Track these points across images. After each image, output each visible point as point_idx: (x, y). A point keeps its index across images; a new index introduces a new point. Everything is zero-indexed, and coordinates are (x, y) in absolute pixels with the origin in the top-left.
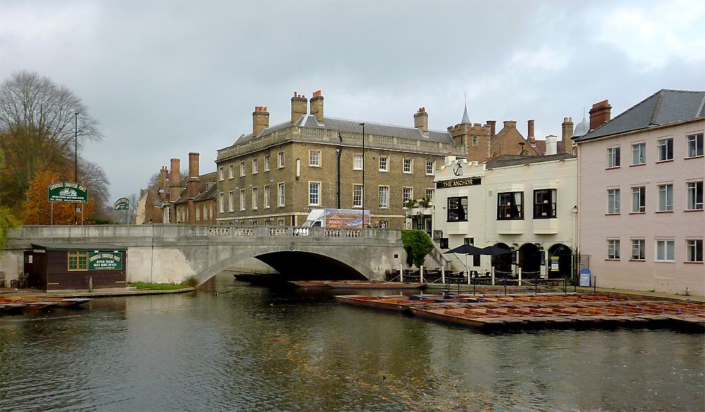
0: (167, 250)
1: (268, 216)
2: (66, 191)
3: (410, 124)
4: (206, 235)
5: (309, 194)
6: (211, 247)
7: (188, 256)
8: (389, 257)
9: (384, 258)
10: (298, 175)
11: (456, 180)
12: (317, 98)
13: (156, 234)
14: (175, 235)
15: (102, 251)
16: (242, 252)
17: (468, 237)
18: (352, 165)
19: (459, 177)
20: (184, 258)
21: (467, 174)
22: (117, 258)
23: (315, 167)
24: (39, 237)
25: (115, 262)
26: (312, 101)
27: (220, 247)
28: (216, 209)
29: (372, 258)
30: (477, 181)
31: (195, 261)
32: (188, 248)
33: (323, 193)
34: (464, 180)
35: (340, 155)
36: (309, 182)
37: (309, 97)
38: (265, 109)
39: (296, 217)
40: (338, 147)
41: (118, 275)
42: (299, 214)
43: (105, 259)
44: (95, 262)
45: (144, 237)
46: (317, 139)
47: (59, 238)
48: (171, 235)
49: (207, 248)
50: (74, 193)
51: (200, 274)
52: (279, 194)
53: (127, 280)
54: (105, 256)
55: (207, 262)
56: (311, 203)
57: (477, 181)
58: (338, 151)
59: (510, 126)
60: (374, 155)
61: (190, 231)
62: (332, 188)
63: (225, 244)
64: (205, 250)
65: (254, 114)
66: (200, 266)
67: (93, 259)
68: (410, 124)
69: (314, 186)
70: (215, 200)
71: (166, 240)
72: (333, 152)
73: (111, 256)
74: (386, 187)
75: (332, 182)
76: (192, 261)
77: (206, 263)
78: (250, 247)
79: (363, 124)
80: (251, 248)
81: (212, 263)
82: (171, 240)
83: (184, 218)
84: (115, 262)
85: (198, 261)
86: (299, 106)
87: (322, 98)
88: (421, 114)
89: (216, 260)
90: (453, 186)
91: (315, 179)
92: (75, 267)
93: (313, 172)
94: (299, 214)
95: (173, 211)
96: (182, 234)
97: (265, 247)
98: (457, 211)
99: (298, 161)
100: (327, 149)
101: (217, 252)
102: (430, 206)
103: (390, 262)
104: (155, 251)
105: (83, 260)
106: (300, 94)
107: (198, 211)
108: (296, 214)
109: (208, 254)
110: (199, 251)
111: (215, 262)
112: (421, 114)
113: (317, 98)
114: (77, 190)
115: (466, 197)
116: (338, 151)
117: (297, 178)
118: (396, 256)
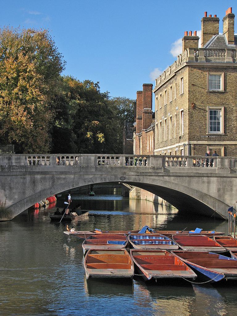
1: (175, 146)
4: (23, 164)
6: (28, 178)
27: (38, 177)
42: (195, 142)
46: (217, 61)
49: (25, 178)
52: (181, 122)
55: (24, 193)
56: (211, 130)
64: (22, 180)
66: (16, 197)
69: (214, 114)
76: (7, 192)
78: (72, 176)
80: (74, 178)
81: (29, 193)
83: (151, 150)
85: (14, 191)
86: (210, 27)
89: (34, 190)
91: (216, 104)
93: (213, 96)
94: (195, 142)
95: (138, 142)
97: (91, 176)
101: (34, 182)
106: (212, 13)
107: (148, 142)
108: (192, 142)
109: (24, 183)
110: (15, 181)
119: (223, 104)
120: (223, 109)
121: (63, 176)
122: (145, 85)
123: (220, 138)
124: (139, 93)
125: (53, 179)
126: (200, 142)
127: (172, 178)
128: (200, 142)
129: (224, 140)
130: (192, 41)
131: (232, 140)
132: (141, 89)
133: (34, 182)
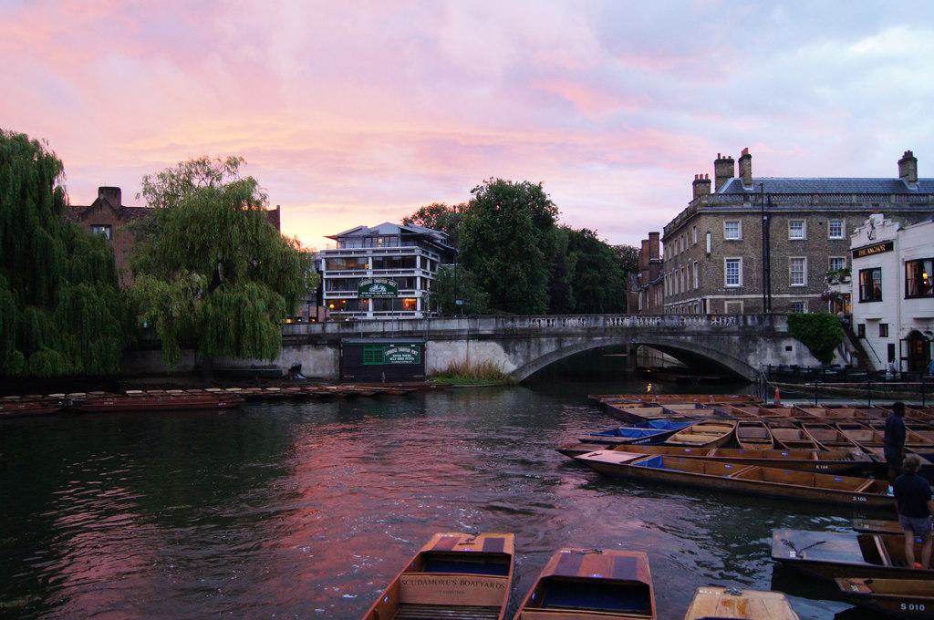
0: (482, 343)
2: (376, 287)
3: (894, 173)
5: (726, 273)
7: (507, 350)
8: (777, 350)
9: (769, 351)
10: (709, 250)
11: (872, 246)
12: (746, 157)
13: (472, 327)
14: (492, 328)
15: (398, 345)
16: (570, 344)
17: (883, 322)
18: (787, 233)
19: (872, 242)
20: (502, 351)
21: (881, 236)
22: (415, 352)
23: (732, 241)
24: (355, 331)
25: (413, 355)
26: (740, 160)
27: (544, 340)
28: (663, 293)
29: (751, 351)
30: (888, 246)
31: (515, 354)
32: (506, 339)
33: (746, 271)
34: (878, 245)
35: (768, 223)
36: (725, 259)
37: (736, 156)
38: (707, 175)
39: (708, 301)
40: (764, 214)
41: (418, 366)
42: (711, 297)
43: (402, 353)
44: (391, 355)
45: (459, 330)
47: (374, 333)
48: (487, 327)
50: (383, 289)
51: (521, 369)
52: (695, 274)
53: (428, 372)
54: (401, 350)
55: (528, 357)
56: (729, 283)
57: (888, 246)
58: (765, 218)
59: (701, 176)
60: (823, 219)
61: (510, 323)
62: (756, 266)
63: (549, 335)
65: (695, 183)
66: (521, 361)
67: (391, 352)
68: (894, 173)
69: (732, 263)
70: (663, 285)
71: (483, 333)
72: (758, 220)
73: (409, 350)
74: (841, 259)
75: (755, 254)
76: (512, 355)
77: (528, 357)
79: (762, 184)
81: (534, 356)
82: (487, 332)
84: (413, 355)
85: (519, 354)
86: (724, 171)
87: (749, 157)
88: (908, 161)
90: (867, 254)
91: (733, 255)
92: (371, 361)
93: (729, 246)
94: (711, 297)
96: (500, 326)
98: (872, 292)
99: (708, 235)
100: (749, 218)
101: (539, 345)
102: (848, 282)
103: (778, 356)
104: (471, 343)
105: (380, 354)
106: (725, 154)
108: (708, 297)
111: (537, 356)
112: (908, 161)
113: (746, 157)
114: (387, 286)
115: (880, 269)
116: (765, 218)
117: (708, 255)
118: (789, 349)
119: (741, 255)
120: (741, 258)
121: (571, 338)
122: (650, 234)
123: (739, 291)
124: (643, 242)
125: (560, 342)
126: (717, 297)
127: (689, 338)
128: (717, 297)
129: (743, 294)
130: (703, 185)
131: (752, 293)
132: (647, 238)
133: (539, 346)
